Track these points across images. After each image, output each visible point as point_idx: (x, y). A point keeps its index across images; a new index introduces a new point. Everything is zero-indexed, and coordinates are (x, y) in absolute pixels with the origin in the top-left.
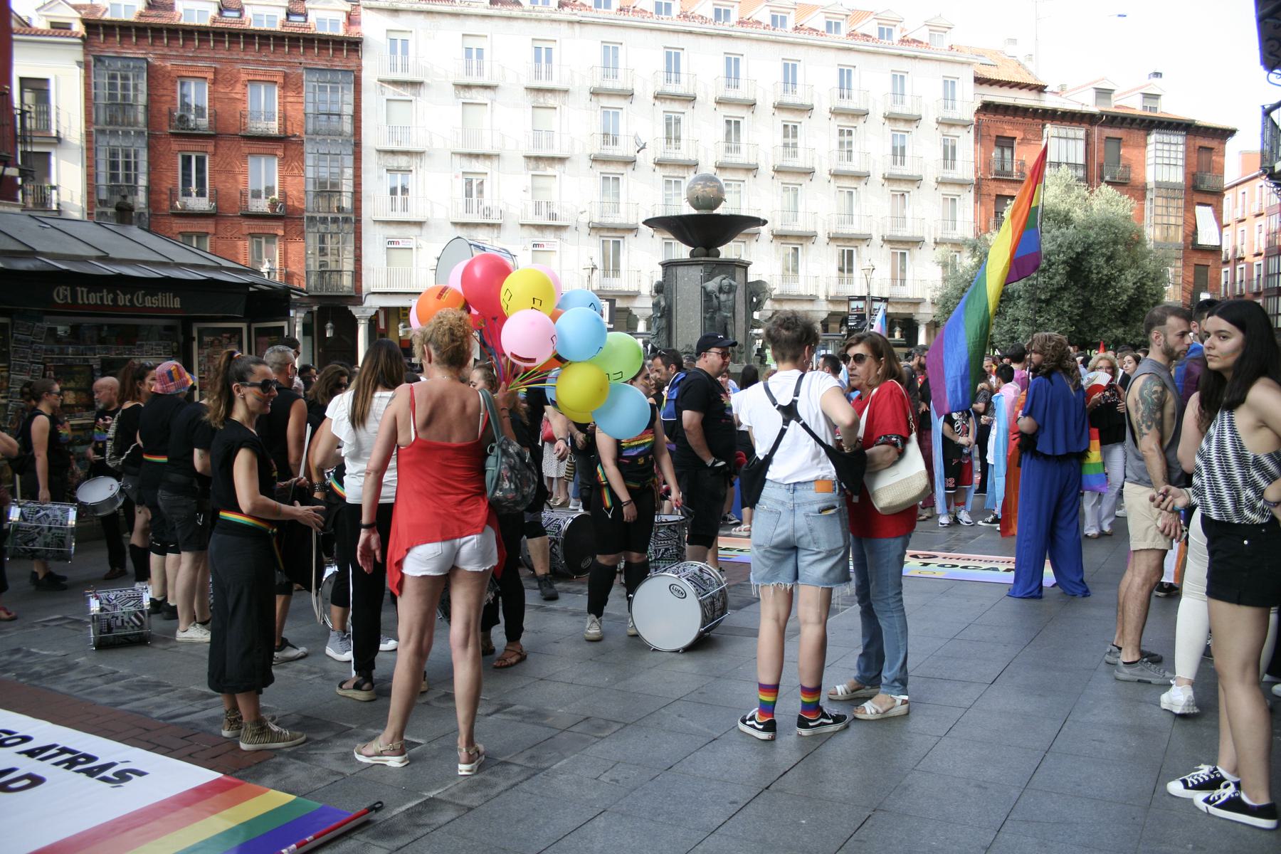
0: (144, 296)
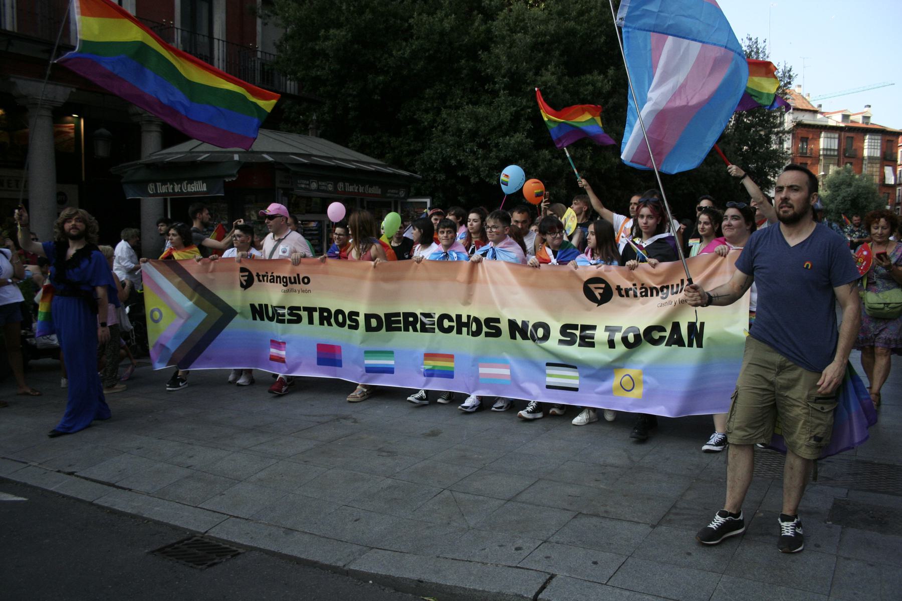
0: (187, 184)
